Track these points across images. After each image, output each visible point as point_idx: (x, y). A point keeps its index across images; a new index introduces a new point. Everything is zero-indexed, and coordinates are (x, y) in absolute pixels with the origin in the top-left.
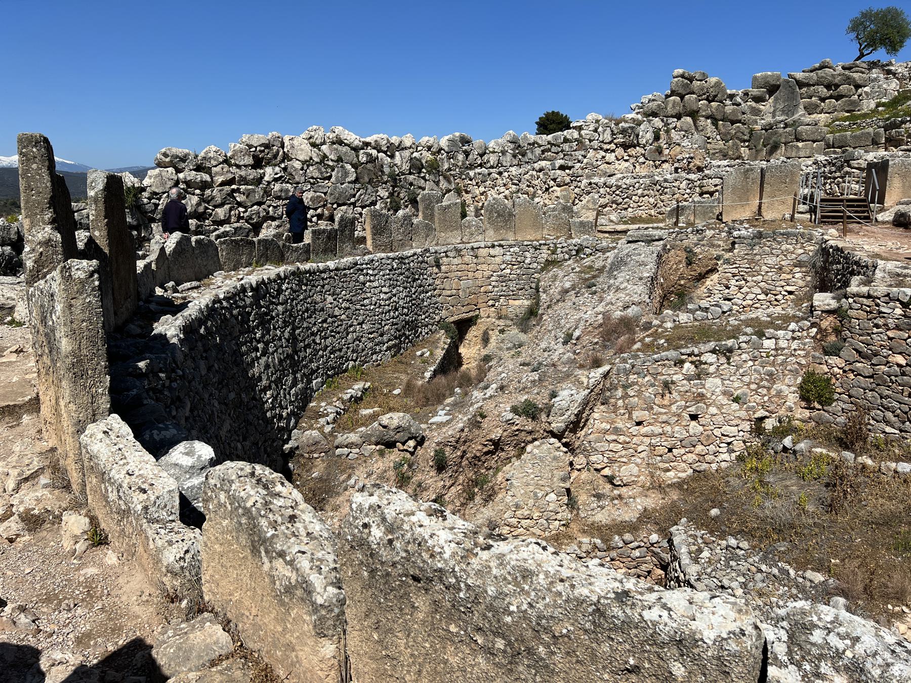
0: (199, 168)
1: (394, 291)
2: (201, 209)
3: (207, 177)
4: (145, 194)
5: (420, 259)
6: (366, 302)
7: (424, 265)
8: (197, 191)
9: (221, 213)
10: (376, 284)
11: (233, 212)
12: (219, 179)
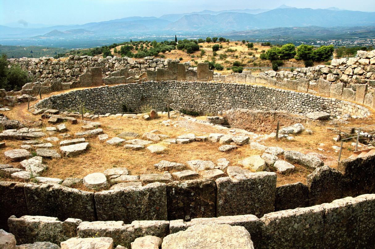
0: (367, 58)
1: (304, 107)
2: (361, 72)
3: (367, 61)
4: (344, 65)
5: (333, 103)
6: (287, 104)
7: (334, 106)
8: (362, 66)
9: (368, 75)
10: (295, 101)
11: (373, 75)
12: (372, 63)
